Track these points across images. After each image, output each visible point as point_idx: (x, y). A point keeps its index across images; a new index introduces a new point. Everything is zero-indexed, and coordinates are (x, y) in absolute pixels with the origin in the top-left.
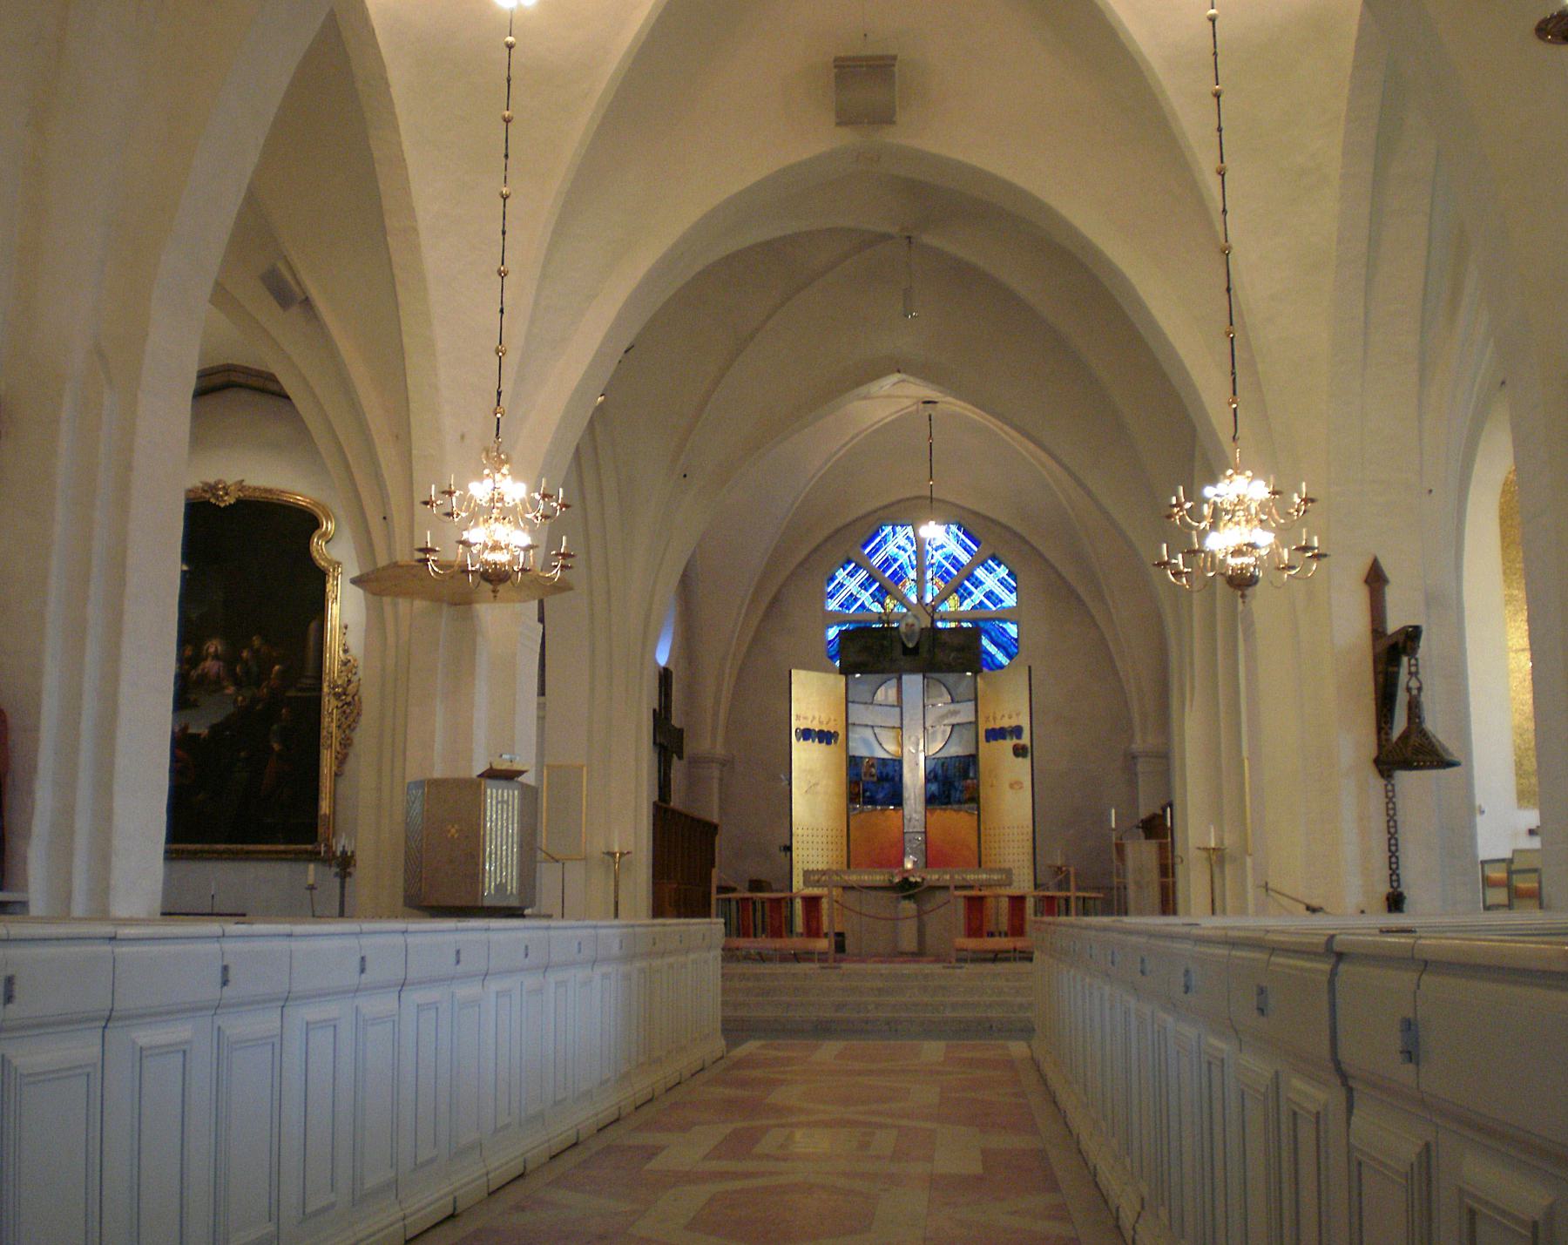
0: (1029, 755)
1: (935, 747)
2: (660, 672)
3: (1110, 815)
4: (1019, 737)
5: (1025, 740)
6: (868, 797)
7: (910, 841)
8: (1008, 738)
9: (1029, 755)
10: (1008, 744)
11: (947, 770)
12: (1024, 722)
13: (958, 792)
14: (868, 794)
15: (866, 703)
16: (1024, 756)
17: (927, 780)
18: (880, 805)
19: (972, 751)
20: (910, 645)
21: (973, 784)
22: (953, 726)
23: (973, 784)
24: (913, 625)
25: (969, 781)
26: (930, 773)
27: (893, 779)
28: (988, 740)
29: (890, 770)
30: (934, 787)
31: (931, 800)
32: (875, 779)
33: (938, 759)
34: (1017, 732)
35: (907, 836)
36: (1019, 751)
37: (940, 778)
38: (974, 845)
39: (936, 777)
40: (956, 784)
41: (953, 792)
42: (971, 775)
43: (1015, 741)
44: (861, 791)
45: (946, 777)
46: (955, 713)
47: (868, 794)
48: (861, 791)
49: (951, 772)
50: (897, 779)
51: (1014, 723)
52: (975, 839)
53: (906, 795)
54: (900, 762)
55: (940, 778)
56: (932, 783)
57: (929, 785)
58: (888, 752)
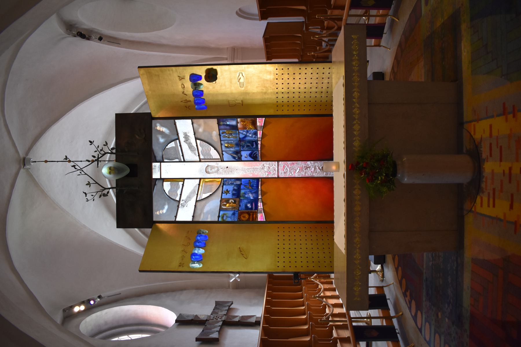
0: (215, 67)
1: (215, 154)
2: (179, 325)
3: (264, 9)
4: (200, 77)
5: (201, 71)
6: (252, 206)
7: (285, 173)
8: (202, 88)
9: (215, 67)
10: (205, 86)
11: (231, 144)
12: (188, 72)
13: (248, 134)
14: (249, 205)
15: (178, 206)
16: (215, 71)
17: (240, 160)
18: (258, 196)
19: (215, 121)
20: (128, 171)
21: (242, 121)
22: (196, 139)
23: (242, 121)
24: (110, 168)
25: (239, 126)
26: (234, 158)
27: (239, 186)
28: (206, 108)
29: (230, 188)
30: (245, 154)
31: (254, 158)
32: (238, 200)
33: (222, 151)
34: (195, 79)
35: (282, 175)
36: (212, 76)
37: (237, 149)
38: (291, 121)
39: (237, 153)
40: (241, 136)
41: (248, 138)
42: (233, 123)
43: (203, 81)
44: (247, 211)
45: (237, 145)
46: (186, 137)
47: (249, 205)
48: (247, 211)
49: (233, 139)
50: (238, 182)
51: (188, 85)
52: (284, 120)
53: (251, 176)
54: (224, 181)
55: (237, 149)
56: (241, 156)
57: (243, 158)
58: (218, 188)
